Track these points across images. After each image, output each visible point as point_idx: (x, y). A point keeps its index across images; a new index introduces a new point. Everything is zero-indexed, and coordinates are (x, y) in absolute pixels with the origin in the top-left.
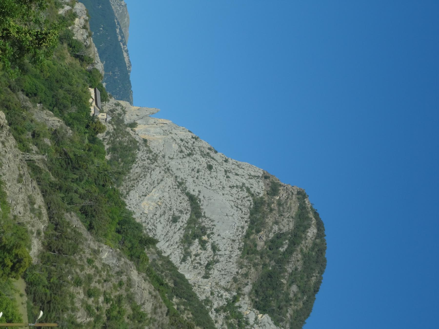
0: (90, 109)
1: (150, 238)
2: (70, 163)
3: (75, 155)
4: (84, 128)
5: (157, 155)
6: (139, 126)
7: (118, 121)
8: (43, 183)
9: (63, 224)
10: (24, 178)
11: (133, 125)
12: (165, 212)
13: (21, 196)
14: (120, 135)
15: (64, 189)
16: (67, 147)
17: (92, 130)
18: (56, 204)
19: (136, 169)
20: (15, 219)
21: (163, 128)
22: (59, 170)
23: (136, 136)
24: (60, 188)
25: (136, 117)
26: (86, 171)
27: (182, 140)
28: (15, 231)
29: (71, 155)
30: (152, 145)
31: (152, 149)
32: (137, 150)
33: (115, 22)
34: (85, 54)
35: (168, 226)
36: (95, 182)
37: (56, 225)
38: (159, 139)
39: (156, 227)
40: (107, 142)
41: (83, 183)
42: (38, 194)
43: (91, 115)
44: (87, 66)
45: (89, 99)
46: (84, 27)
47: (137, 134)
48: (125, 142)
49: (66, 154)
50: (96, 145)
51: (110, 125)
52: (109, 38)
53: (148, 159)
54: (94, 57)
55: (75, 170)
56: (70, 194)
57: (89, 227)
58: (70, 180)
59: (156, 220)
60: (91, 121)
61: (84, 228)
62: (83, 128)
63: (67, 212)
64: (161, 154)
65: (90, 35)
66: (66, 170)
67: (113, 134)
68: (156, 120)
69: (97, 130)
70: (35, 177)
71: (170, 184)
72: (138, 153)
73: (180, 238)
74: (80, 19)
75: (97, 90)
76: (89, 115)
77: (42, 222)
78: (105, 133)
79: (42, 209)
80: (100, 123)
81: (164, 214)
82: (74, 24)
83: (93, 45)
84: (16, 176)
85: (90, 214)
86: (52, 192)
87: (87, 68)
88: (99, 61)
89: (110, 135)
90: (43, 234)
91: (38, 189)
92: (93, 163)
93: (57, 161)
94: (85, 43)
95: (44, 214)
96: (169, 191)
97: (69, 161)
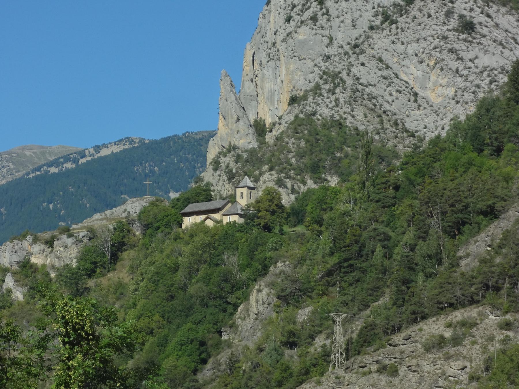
0: (229, 224)
1: (510, 80)
2: (350, 263)
3: (332, 254)
4: (272, 234)
5: (324, 73)
6: (261, 115)
7: (251, 163)
8: (396, 321)
9: (485, 272)
10: (386, 362)
11: (260, 129)
12: (452, 51)
13: (427, 367)
14: (282, 156)
15: (407, 274)
16: (314, 272)
17: (274, 217)
18: (440, 290)
19: (358, 119)
20: (478, 378)
21: (264, 62)
22: (365, 286)
23: (283, 121)
24: (406, 282)
25: (241, 122)
26: (366, 228)
27: (288, 19)
28: (504, 377)
29: (333, 261)
30: (302, 85)
31: (312, 85)
32: (315, 118)
33: (36, 178)
34: (109, 239)
35: (483, 40)
36: (389, 207)
37: (487, 287)
38: (287, 69)
39: (485, 68)
40: (301, 185)
41: (391, 234)
42: (421, 330)
43: (241, 221)
44: (134, 235)
45: (206, 227)
46: (50, 243)
47: (280, 118)
48: (298, 145)
49: (329, 273)
50: (308, 208)
51: (262, 179)
52: (71, 189)
53: (334, 93)
54: (113, 219)
55: (365, 251)
56: (418, 260)
57: (490, 216)
58: (387, 262)
59: (469, 68)
60: (256, 220)
61: (492, 226)
62: (272, 240)
63: (458, 265)
64: (322, 64)
65: (67, 231)
66: (364, 272)
67: (282, 172)
68: (247, 78)
69: (274, 207)
70: (385, 339)
71: (387, 42)
72: (320, 115)
73: (508, 13)
74: (31, 254)
75: (187, 210)
76: (242, 225)
77: (482, 320)
78: (281, 190)
79: (455, 321)
80: (257, 202)
81: (456, 51)
82: (44, 266)
83: (87, 222)
84: (384, 379)
85: (460, 215)
86: (416, 299)
87: (138, 233)
88: (123, 207)
89: (285, 177)
90: (508, 317)
91: (410, 330)
92: (346, 214)
93: (346, 292)
94: (85, 240)
95: (465, 315)
96: (403, 43)
97: (346, 264)
